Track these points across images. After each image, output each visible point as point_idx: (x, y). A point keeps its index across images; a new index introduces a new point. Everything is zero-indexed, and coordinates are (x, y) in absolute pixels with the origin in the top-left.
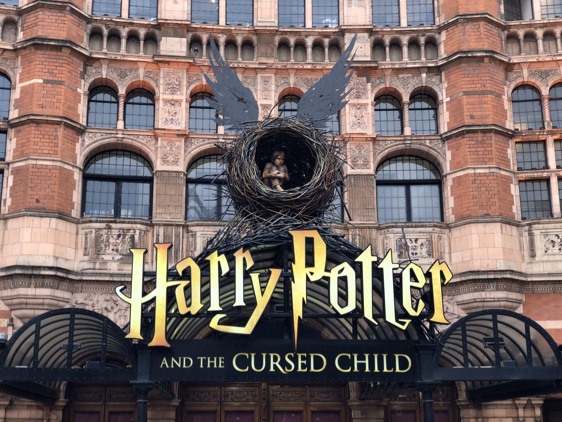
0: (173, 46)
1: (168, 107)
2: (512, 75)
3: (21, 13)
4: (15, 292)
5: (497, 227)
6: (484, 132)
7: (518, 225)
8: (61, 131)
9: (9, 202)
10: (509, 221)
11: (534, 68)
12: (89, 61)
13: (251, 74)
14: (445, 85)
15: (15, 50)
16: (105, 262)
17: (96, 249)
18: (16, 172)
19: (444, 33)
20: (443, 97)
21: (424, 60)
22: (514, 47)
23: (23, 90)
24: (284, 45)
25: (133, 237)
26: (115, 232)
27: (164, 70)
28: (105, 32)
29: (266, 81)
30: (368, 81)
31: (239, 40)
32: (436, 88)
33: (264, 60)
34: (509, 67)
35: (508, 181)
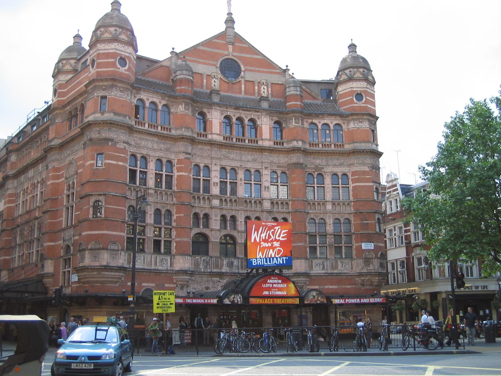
0: (216, 202)
1: (215, 222)
2: (308, 216)
3: (174, 192)
4: (179, 277)
5: (303, 261)
6: (302, 233)
7: (308, 260)
8: (189, 230)
9: (175, 251)
10: (306, 259)
11: (314, 214)
12: (193, 207)
13: (237, 211)
14: (291, 218)
15: (174, 204)
16: (200, 268)
17: (197, 264)
18: (177, 242)
19: (291, 202)
20: (290, 221)
21: (285, 210)
22: (309, 207)
23: (177, 217)
24: (246, 201)
25: (207, 261)
26: (202, 260)
27: (213, 210)
28: (196, 197)
29: (241, 214)
30: (270, 215)
31: (233, 200)
32: (288, 218)
33: (241, 207)
34: (308, 213)
35: (306, 247)
